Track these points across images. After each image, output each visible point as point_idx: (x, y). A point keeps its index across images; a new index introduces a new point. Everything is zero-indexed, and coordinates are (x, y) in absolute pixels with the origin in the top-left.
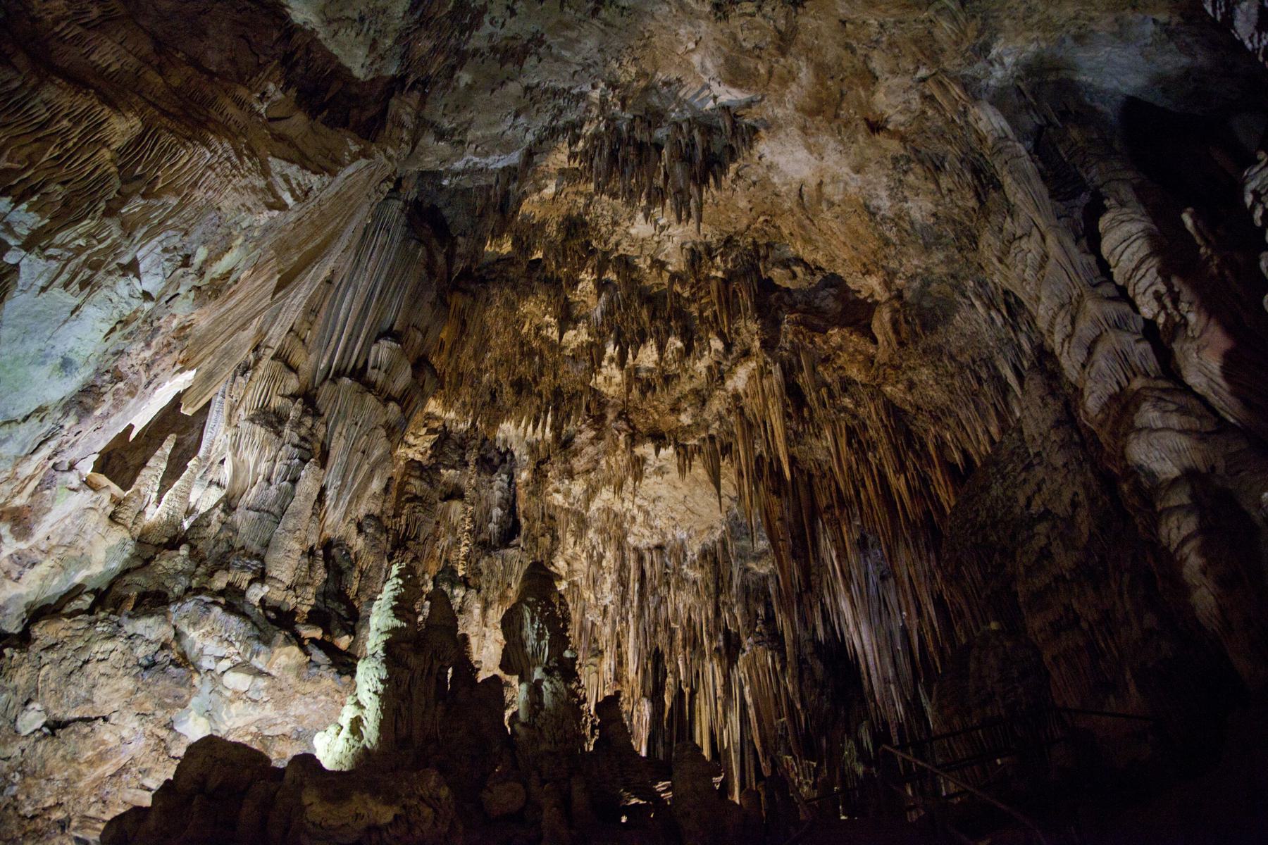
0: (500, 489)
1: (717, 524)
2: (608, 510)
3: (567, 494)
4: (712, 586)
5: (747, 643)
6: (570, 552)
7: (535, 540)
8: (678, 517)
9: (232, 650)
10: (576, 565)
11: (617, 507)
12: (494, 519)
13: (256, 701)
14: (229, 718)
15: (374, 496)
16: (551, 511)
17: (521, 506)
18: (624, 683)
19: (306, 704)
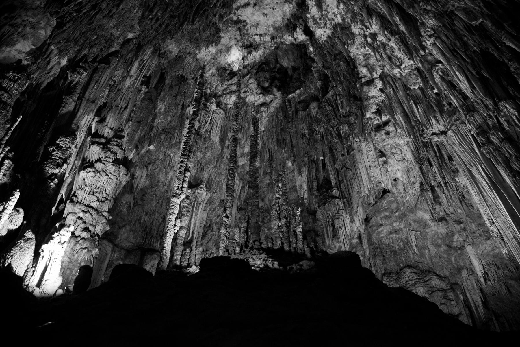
7: (338, 74)
10: (372, 60)
18: (477, 107)
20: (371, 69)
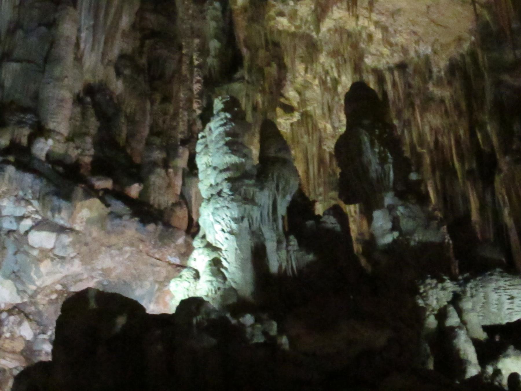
0: (215, 18)
1: (466, 35)
2: (340, 30)
3: (293, 16)
4: (463, 105)
5: (504, 162)
6: (300, 80)
7: (261, 70)
8: (420, 30)
9: (30, 208)
10: (308, 94)
11: (351, 25)
12: (213, 53)
13: (63, 258)
14: (39, 277)
15: (124, 34)
16: (276, 38)
17: (241, 34)
19: (112, 257)
20: (303, 102)
